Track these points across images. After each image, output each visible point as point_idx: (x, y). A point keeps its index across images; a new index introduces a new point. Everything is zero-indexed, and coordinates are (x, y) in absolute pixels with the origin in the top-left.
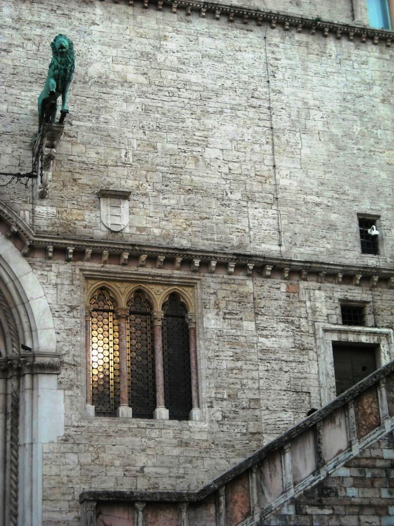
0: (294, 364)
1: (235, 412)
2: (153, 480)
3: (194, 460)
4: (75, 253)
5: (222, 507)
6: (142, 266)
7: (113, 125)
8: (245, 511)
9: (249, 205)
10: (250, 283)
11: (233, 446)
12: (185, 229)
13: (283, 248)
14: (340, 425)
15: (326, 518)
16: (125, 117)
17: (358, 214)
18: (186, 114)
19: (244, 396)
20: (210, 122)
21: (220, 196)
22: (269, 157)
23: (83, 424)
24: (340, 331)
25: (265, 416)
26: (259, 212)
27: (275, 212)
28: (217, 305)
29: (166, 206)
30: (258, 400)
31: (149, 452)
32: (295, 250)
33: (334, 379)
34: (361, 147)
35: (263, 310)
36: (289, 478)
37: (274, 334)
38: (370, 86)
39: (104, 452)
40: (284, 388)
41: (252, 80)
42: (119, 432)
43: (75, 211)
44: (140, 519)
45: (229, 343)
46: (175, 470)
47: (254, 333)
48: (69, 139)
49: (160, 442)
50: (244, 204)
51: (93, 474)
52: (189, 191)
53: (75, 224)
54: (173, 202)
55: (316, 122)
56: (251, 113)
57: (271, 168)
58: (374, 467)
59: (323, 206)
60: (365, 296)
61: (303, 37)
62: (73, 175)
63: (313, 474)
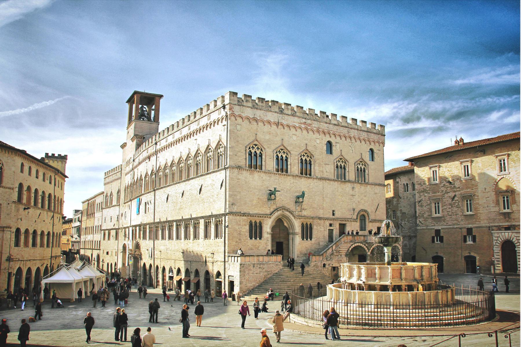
20: (316, 197)
42: (305, 242)
61: (328, 181)
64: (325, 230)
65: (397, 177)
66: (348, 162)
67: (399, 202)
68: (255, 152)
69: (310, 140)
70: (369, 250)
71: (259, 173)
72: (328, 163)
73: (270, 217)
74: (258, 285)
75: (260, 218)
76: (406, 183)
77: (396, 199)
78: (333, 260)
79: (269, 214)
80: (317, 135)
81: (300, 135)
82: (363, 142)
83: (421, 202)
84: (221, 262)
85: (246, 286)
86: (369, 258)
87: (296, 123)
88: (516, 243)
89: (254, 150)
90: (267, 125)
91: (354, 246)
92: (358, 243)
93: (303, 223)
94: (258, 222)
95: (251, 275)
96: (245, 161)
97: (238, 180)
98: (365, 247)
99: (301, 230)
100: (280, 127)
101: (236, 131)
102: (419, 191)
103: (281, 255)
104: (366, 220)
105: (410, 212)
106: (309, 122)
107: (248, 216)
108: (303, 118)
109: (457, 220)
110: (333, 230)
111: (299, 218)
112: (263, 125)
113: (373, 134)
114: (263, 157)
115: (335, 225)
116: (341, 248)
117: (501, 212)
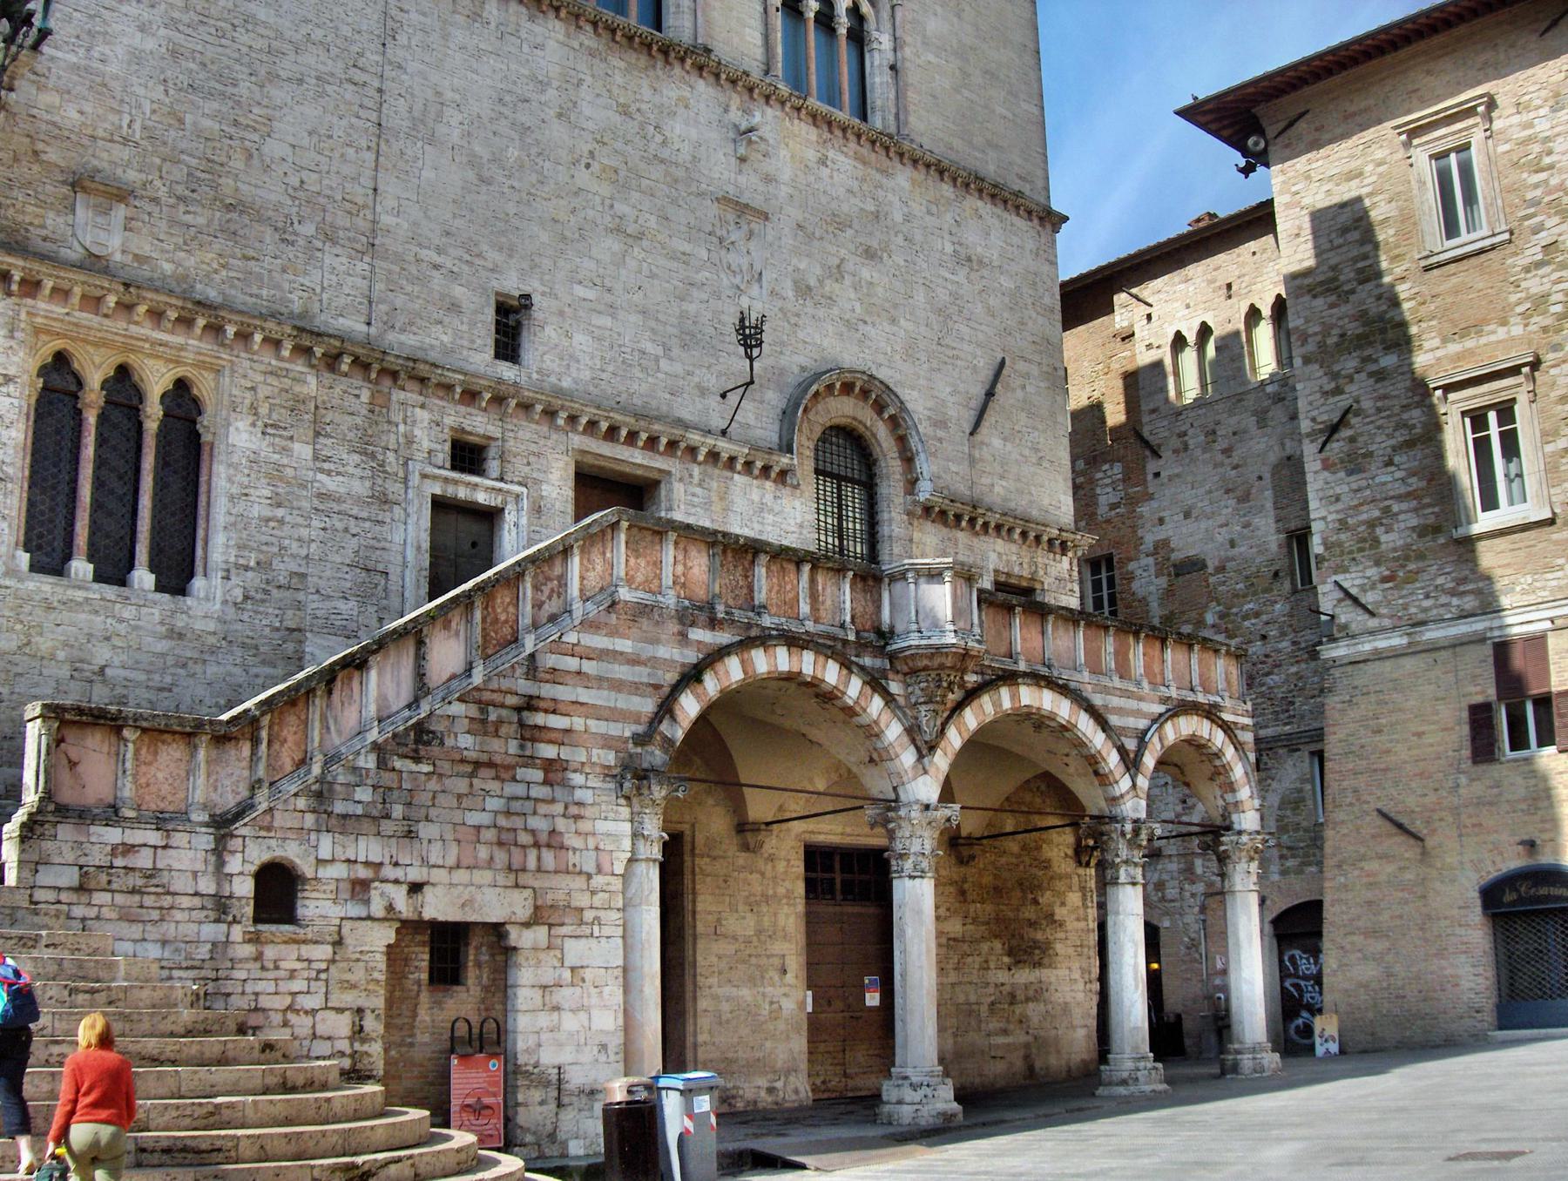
0: (367, 525)
1: (266, 592)
2: (119, 691)
3: (190, 663)
4: (23, 281)
5: (264, 746)
6: (137, 323)
7: (113, 68)
8: (298, 756)
9: (327, 248)
10: (312, 380)
11: (256, 647)
12: (216, 272)
13: (373, 330)
14: (457, 634)
15: (423, 778)
16: (136, 57)
17: (497, 294)
18: (241, 72)
19: (282, 566)
20: (279, 94)
21: (280, 225)
22: (369, 173)
23: (7, 582)
24: (446, 480)
25: (314, 603)
26: (342, 263)
27: (366, 267)
28: (254, 410)
29: (189, 226)
30: (303, 576)
31: (116, 641)
32: (392, 337)
33: (427, 556)
34: (516, 184)
35: (328, 428)
36: (372, 710)
37: (341, 469)
38: (543, 85)
39: (41, 634)
40: (348, 561)
41: (357, 37)
43: (30, 209)
44: (129, 755)
45: (268, 475)
46: (157, 677)
47: (311, 464)
48: (33, 77)
49: (136, 628)
50: (319, 244)
51: (19, 670)
52: (230, 207)
53: (27, 230)
54: (201, 221)
55: (452, 128)
56: (349, 92)
57: (370, 192)
58: (503, 706)
59: (443, 271)
60: (490, 428)
62: (33, 143)
63: (409, 706)
65: (1120, 298)
67: (1144, 483)
70: (925, 749)
76: (1196, 326)
77: (1118, 468)
78: (425, 830)
83: (1345, 433)
91: (733, 671)
92: (794, 642)
93: (61, 360)
98: (877, 703)
102: (1322, 345)
105: (1242, 549)
110: (490, 517)
115: (519, 468)
116: (555, 676)
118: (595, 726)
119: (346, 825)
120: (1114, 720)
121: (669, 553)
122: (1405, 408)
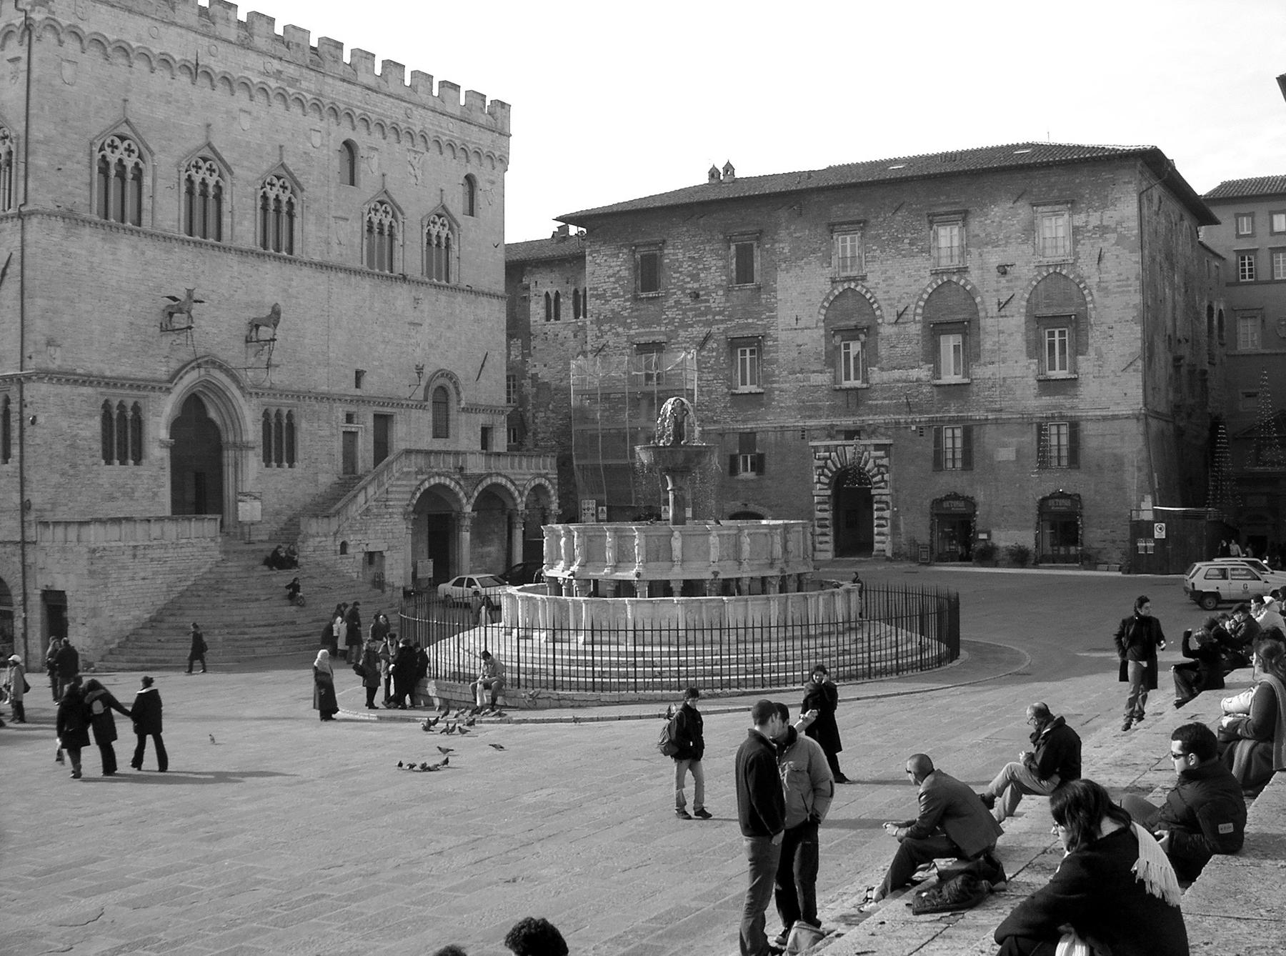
25: (320, 466)
61: (341, 275)
64: (333, 435)
66: (402, 214)
68: (120, 160)
69: (293, 134)
71: (135, 238)
72: (344, 215)
73: (168, 390)
74: (147, 616)
75: (135, 392)
79: (165, 377)
80: (313, 119)
81: (263, 114)
82: (448, 153)
84: (17, 543)
85: (113, 623)
86: (467, 522)
87: (252, 70)
88: (874, 476)
89: (117, 155)
90: (162, 75)
91: (427, 485)
92: (439, 475)
94: (129, 403)
95: (127, 583)
96: (87, 193)
97: (66, 260)
98: (457, 488)
99: (261, 434)
100: (202, 81)
101: (58, 82)
102: (598, 318)
103: (214, 516)
104: (451, 405)
106: (291, 70)
107: (99, 383)
108: (274, 57)
109: (714, 410)
110: (354, 434)
111: (257, 394)
112: (147, 69)
113: (476, 129)
114: (147, 181)
115: (361, 419)
117: (837, 387)
118: (399, 503)
119: (355, 533)
120: (517, 483)
121: (413, 457)
122: (624, 348)
